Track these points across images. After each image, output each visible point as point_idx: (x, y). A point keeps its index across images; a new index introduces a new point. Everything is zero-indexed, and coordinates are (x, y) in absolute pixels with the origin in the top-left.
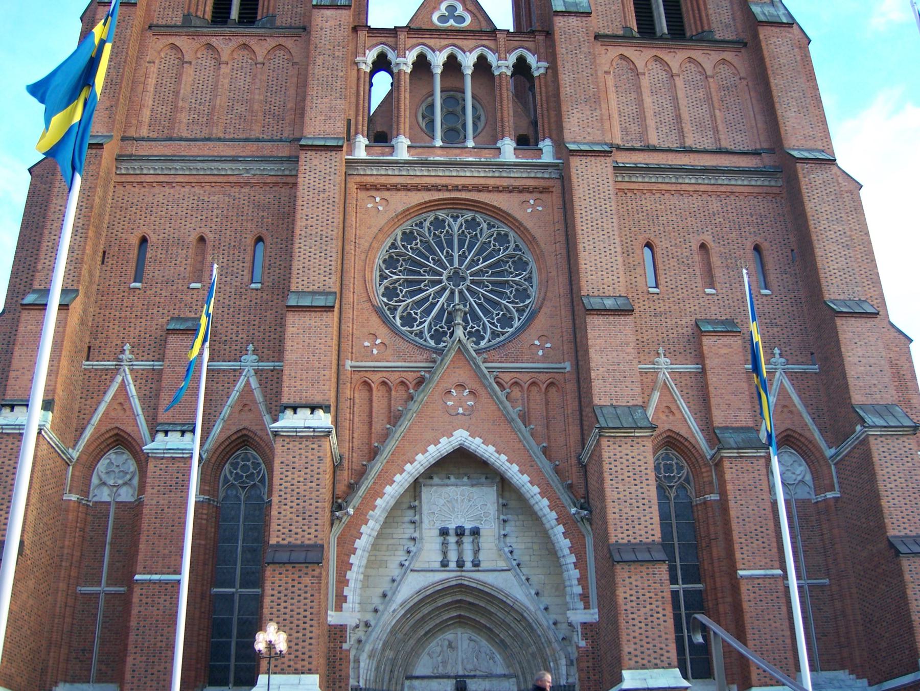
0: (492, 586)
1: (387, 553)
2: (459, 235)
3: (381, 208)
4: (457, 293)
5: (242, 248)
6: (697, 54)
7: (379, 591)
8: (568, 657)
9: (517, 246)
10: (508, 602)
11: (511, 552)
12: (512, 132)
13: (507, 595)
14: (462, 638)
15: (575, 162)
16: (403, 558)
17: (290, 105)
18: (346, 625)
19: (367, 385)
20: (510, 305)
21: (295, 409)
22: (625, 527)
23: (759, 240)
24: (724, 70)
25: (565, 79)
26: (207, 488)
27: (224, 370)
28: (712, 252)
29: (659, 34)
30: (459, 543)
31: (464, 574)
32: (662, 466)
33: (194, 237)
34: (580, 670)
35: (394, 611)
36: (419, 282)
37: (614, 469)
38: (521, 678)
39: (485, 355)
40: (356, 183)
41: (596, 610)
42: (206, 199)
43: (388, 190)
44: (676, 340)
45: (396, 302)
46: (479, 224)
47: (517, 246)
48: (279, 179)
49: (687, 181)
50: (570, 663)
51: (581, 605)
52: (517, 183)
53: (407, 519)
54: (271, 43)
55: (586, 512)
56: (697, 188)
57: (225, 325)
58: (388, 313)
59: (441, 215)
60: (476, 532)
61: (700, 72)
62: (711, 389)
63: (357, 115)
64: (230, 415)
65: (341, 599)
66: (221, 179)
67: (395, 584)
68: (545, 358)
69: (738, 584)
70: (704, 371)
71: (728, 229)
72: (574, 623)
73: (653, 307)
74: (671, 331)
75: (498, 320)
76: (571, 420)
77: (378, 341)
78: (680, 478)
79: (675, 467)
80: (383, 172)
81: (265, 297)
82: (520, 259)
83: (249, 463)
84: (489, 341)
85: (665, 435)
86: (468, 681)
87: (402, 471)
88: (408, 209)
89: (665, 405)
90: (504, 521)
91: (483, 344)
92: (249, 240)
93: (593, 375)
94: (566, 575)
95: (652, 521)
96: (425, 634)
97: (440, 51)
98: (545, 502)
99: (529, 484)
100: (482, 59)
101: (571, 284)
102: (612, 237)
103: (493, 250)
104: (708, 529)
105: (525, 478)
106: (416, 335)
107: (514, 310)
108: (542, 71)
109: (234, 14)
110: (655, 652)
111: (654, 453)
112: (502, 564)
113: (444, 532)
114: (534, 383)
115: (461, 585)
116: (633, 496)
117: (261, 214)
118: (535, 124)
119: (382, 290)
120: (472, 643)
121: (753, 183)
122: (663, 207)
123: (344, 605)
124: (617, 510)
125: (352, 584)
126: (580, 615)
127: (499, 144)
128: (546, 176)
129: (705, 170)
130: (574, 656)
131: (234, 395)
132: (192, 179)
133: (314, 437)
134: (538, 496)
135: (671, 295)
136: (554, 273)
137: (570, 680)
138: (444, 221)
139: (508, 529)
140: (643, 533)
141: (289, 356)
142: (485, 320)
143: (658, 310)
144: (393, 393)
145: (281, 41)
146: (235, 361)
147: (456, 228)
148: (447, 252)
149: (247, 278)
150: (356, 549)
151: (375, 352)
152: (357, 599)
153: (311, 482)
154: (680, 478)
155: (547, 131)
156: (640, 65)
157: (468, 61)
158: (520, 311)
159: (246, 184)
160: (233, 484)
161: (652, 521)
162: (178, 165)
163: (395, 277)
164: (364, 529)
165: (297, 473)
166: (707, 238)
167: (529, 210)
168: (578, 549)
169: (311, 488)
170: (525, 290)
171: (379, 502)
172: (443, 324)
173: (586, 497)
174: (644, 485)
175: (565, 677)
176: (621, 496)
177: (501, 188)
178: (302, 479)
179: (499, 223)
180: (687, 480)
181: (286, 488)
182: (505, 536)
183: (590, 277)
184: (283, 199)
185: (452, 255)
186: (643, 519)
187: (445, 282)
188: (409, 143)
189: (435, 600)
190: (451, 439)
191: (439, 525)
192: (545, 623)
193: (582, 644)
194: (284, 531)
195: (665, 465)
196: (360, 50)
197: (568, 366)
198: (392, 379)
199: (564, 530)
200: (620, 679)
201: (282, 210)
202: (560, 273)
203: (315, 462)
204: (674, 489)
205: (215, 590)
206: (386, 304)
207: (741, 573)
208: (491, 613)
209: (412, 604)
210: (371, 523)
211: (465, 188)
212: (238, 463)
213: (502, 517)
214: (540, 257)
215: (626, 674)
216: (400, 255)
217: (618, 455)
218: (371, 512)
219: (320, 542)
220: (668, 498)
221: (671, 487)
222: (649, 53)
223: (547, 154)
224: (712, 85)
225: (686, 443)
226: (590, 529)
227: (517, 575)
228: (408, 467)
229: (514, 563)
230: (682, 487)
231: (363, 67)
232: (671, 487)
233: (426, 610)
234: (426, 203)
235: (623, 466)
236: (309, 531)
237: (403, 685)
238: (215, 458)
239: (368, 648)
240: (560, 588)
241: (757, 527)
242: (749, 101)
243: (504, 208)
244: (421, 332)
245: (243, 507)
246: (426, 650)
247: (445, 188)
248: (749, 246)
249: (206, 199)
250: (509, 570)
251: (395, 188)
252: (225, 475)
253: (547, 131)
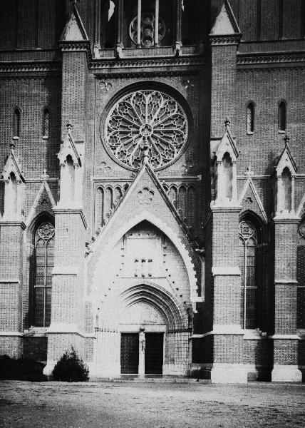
119: (108, 138)
137: (190, 327)
193: (196, 312)
216: (118, 117)
244: (128, 161)
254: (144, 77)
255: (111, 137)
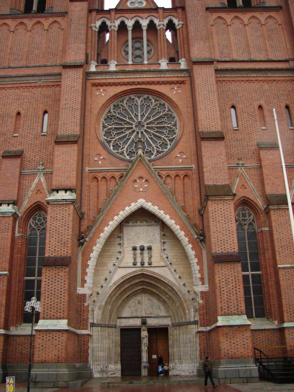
0: (158, 274)
1: (107, 259)
2: (141, 106)
3: (103, 94)
4: (140, 133)
5: (38, 116)
6: (256, 14)
7: (103, 278)
8: (194, 308)
9: (169, 110)
10: (165, 281)
11: (167, 258)
12: (166, 56)
13: (165, 278)
14: (145, 299)
15: (197, 69)
16: (115, 262)
17: (60, 48)
18: (86, 294)
19: (95, 178)
20: (166, 138)
21: (57, 191)
22: (220, 245)
23: (288, 103)
24: (270, 21)
25: (191, 28)
26: (21, 230)
27: (29, 174)
28: (264, 109)
29: (238, 6)
30: (142, 254)
31: (144, 268)
32: (241, 214)
33: (15, 113)
34: (200, 315)
35: (111, 287)
36: (122, 128)
37: (214, 216)
38: (173, 317)
39: (153, 163)
40: (91, 83)
41: (208, 285)
42: (21, 95)
43: (107, 86)
44: (247, 153)
45: (111, 138)
46: (150, 100)
47: (169, 110)
48: (55, 84)
49: (252, 75)
50: (196, 311)
51: (200, 283)
52: (168, 80)
53: (117, 243)
54: (51, 20)
55: (202, 238)
56: (257, 79)
57: (29, 153)
58: (107, 144)
59: (132, 96)
60: (150, 248)
61: (258, 23)
62: (264, 175)
63: (92, 51)
64: (31, 195)
65: (84, 282)
66: (28, 85)
67: (111, 274)
68: (183, 163)
69: (278, 271)
70: (261, 167)
71: (272, 98)
72: (197, 292)
73: (236, 137)
74: (244, 148)
75: (160, 145)
76: (195, 193)
77: (102, 158)
78: (250, 220)
79: (247, 214)
80: (104, 78)
81: (48, 139)
82: (171, 116)
83: (41, 218)
84: (156, 156)
85: (242, 199)
86: (147, 319)
87: (112, 220)
88: (116, 94)
89: (242, 184)
90: (164, 243)
91: (152, 157)
92: (41, 113)
93: (205, 170)
94: (193, 268)
95: (233, 242)
96: (127, 297)
97: (131, 19)
98: (183, 233)
99: (175, 225)
100: (151, 23)
101: (195, 127)
102: (214, 103)
103: (158, 112)
104: (263, 244)
105: (173, 221)
106: (120, 154)
107: (168, 141)
108: (180, 26)
109: (35, 8)
110: (234, 307)
111: (235, 209)
112: (162, 264)
113: (134, 249)
114: (177, 176)
115: (143, 274)
116: (224, 229)
117: (46, 100)
118: (177, 52)
120: (150, 301)
121: (285, 75)
122: (240, 88)
123: (85, 284)
124: (216, 237)
125: (89, 275)
126: (201, 288)
127: (160, 62)
128: (183, 75)
129: (260, 70)
130: (197, 308)
131: (34, 186)
132: (14, 86)
133: (66, 204)
134: (179, 230)
135: (245, 131)
136: (187, 122)
138: (134, 99)
139: (166, 247)
140: (229, 247)
141: (56, 166)
142: (154, 145)
143: (238, 138)
144: (109, 182)
145: (56, 19)
146: (34, 169)
147: (139, 102)
148: (135, 114)
149: (40, 130)
150: (91, 257)
151: (100, 163)
152: (91, 282)
153: (65, 226)
154: (250, 220)
155: (183, 55)
156: (229, 21)
157: (144, 23)
158: (171, 141)
159: (40, 86)
160: (34, 228)
161: (233, 242)
162: (8, 80)
163: (110, 127)
164: (94, 248)
165: (58, 222)
166: (262, 103)
167: (175, 92)
168: (199, 256)
169: (65, 229)
170: (173, 130)
171: (102, 235)
172: (133, 148)
173: (203, 230)
174: (230, 224)
175: (193, 317)
176: (218, 229)
177: (161, 82)
178: (60, 225)
179: (160, 99)
180: (253, 221)
181: (53, 229)
182: (164, 250)
183: (203, 123)
184: (57, 92)
185: (137, 116)
186: (229, 240)
187: (134, 128)
188: (116, 63)
189: (130, 282)
190: (136, 204)
191: (132, 245)
192: (184, 291)
193: (201, 302)
194: (51, 250)
195: (243, 213)
196: (93, 21)
197: (194, 166)
198: (108, 175)
199: (192, 247)
200: (217, 321)
201: (56, 98)
202: (190, 121)
203: (67, 216)
204: (246, 225)
205: (26, 278)
206: (106, 140)
207: (279, 266)
208: (158, 287)
209: (119, 283)
210: (98, 245)
211: (143, 83)
212: (36, 218)
213: (162, 241)
214: (180, 114)
215: (219, 318)
216: (112, 116)
217: (217, 209)
218: (98, 240)
219: (69, 255)
220: (244, 230)
221: (245, 224)
222: (233, 15)
223: (183, 65)
224: (264, 29)
225: (252, 203)
226: (204, 245)
227: (169, 269)
228: (116, 218)
229: (169, 263)
230: (250, 224)
231: (94, 28)
232: (245, 224)
233: (126, 286)
234: (125, 91)
235: (219, 214)
236: (64, 250)
237: (116, 321)
238: (25, 216)
239: (98, 304)
240: (190, 274)
241: (287, 243)
242: (283, 36)
243: (162, 92)
244: (123, 153)
245: (38, 239)
246: (128, 304)
247: (134, 83)
248: (283, 106)
249: (21, 95)
250: (166, 266)
251: (110, 84)
252: (30, 225)
253: (183, 55)
254: (136, 85)
255: (106, 132)
